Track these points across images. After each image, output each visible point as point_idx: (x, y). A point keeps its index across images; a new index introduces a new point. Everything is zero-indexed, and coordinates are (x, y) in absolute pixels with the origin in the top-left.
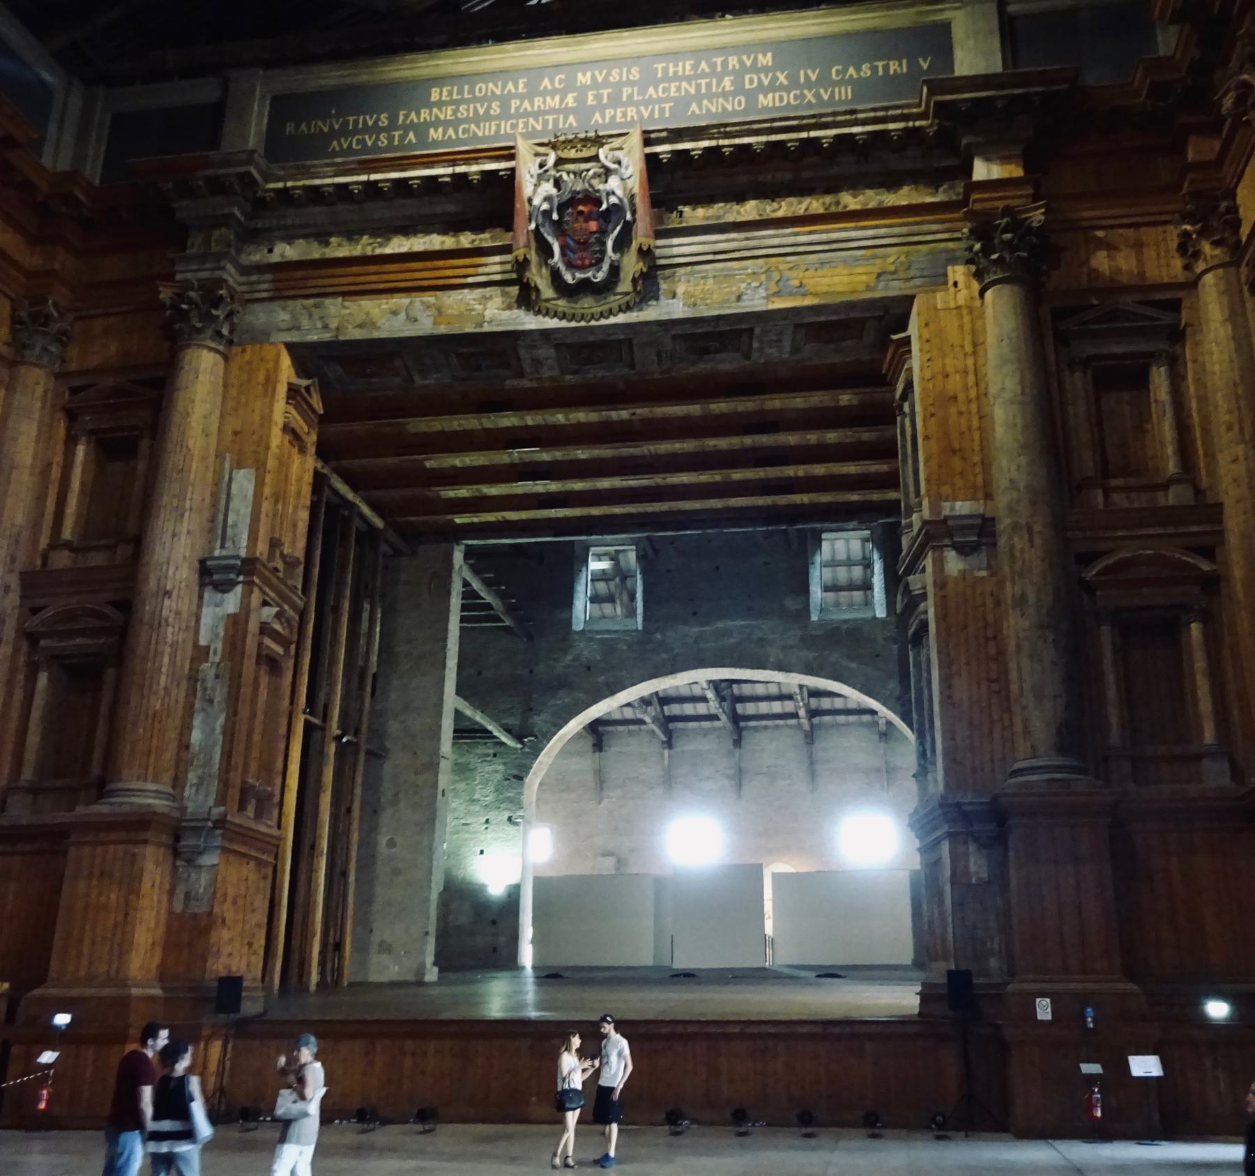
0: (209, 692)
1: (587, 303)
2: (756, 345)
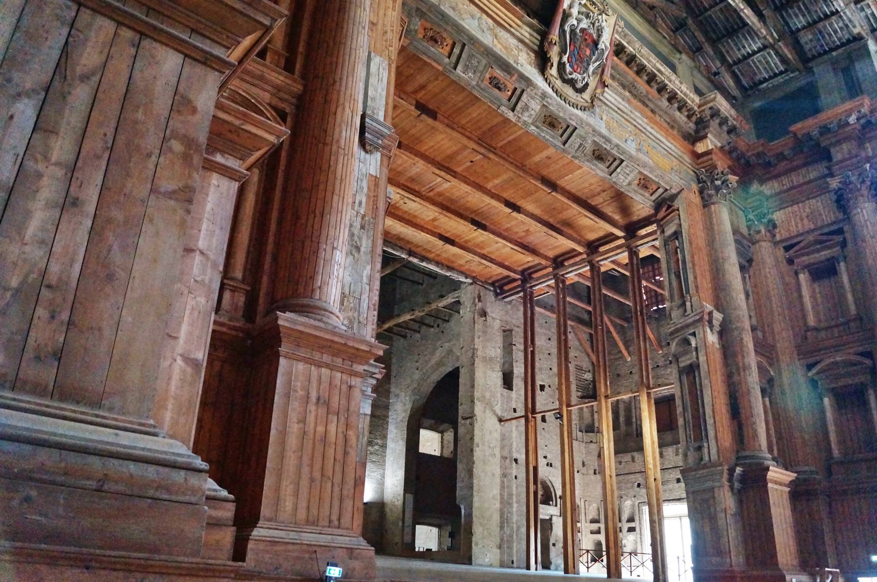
0: (356, 238)
1: (569, 91)
2: (618, 170)
